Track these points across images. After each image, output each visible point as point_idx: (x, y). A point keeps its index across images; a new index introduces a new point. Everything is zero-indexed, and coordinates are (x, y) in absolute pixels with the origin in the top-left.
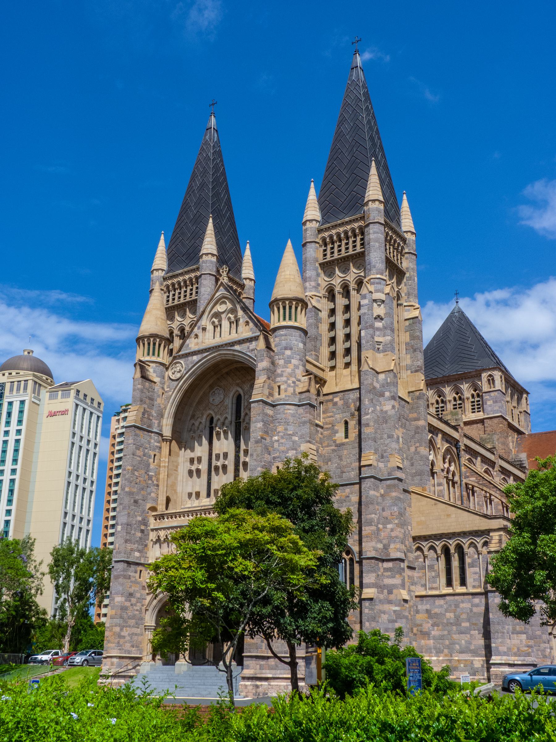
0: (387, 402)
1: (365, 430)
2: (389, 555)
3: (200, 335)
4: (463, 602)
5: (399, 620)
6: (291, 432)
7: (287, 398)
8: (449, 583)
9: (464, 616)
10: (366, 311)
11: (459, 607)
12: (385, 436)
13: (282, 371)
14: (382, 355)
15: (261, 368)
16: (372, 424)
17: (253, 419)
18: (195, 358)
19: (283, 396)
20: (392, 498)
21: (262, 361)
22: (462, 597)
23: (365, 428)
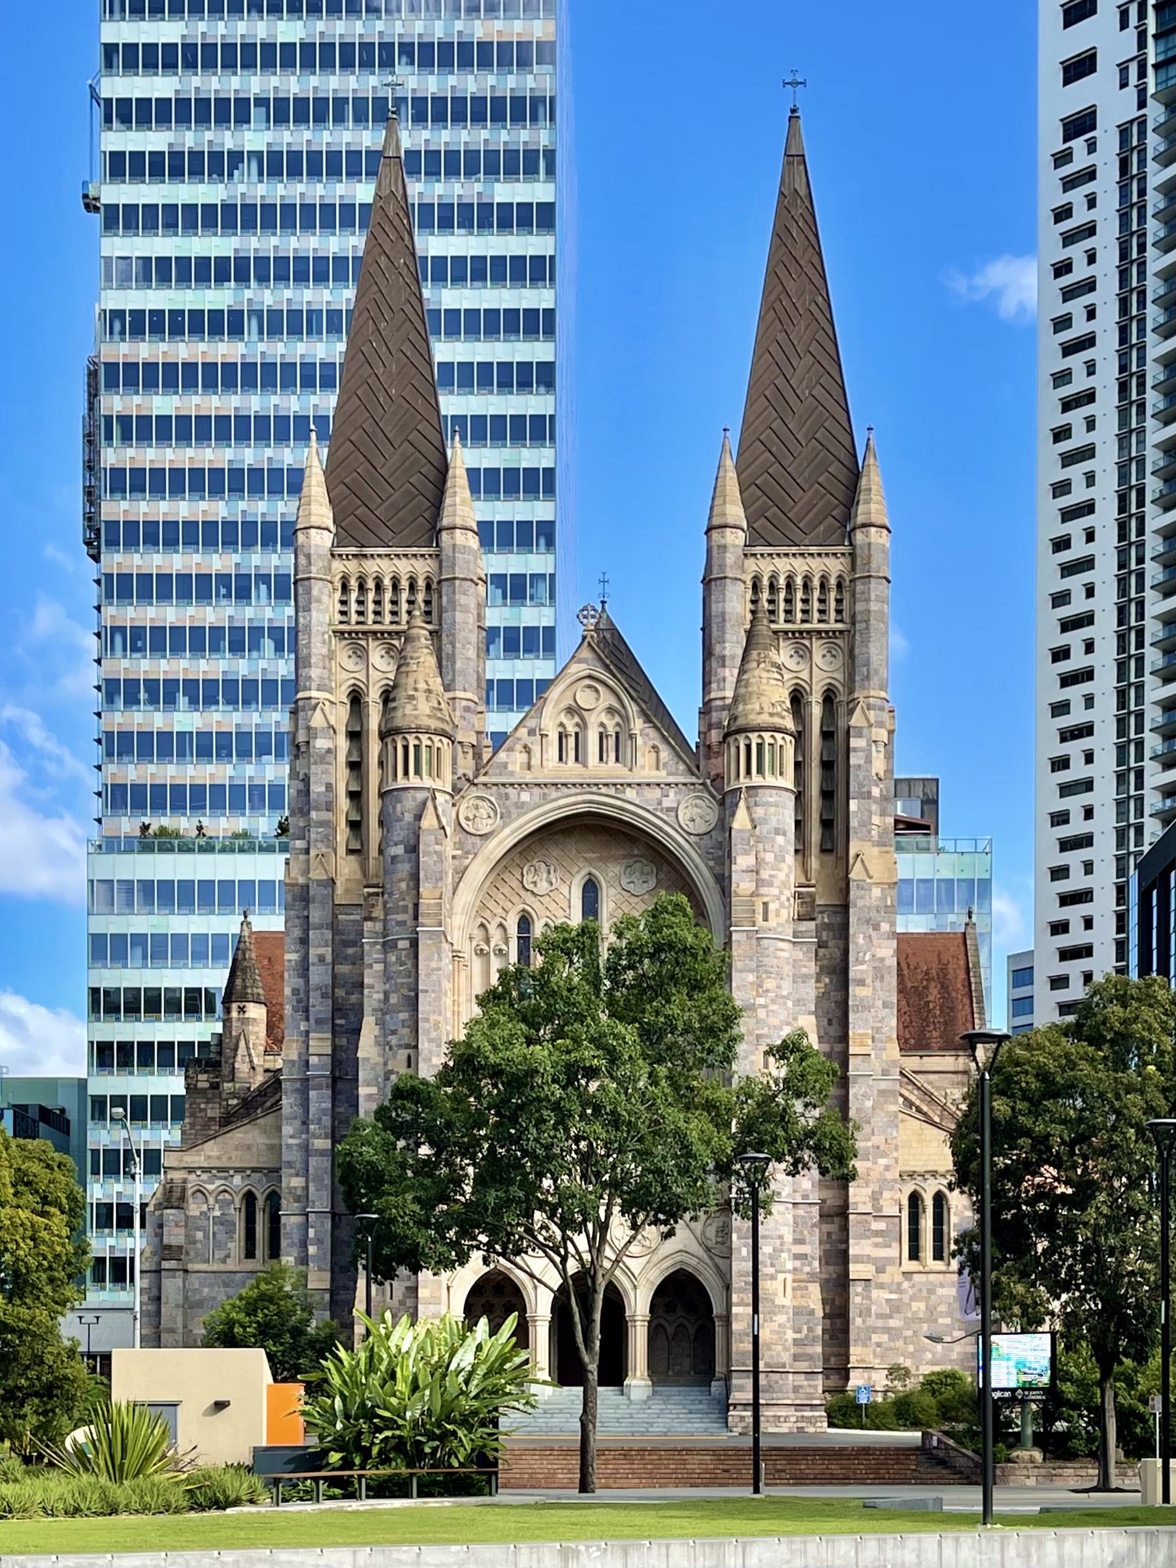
0: (886, 942)
1: (855, 991)
2: (880, 1209)
3: (536, 749)
4: (942, 1286)
5: (895, 1315)
6: (785, 993)
7: (780, 929)
8: (914, 1254)
9: (943, 1308)
10: (862, 762)
11: (934, 1293)
12: (879, 1003)
13: (770, 876)
14: (876, 850)
15: (744, 868)
16: (869, 981)
17: (737, 964)
18: (525, 796)
19: (772, 922)
20: (887, 1113)
21: (746, 852)
22: (941, 1276)
23: (858, 988)
